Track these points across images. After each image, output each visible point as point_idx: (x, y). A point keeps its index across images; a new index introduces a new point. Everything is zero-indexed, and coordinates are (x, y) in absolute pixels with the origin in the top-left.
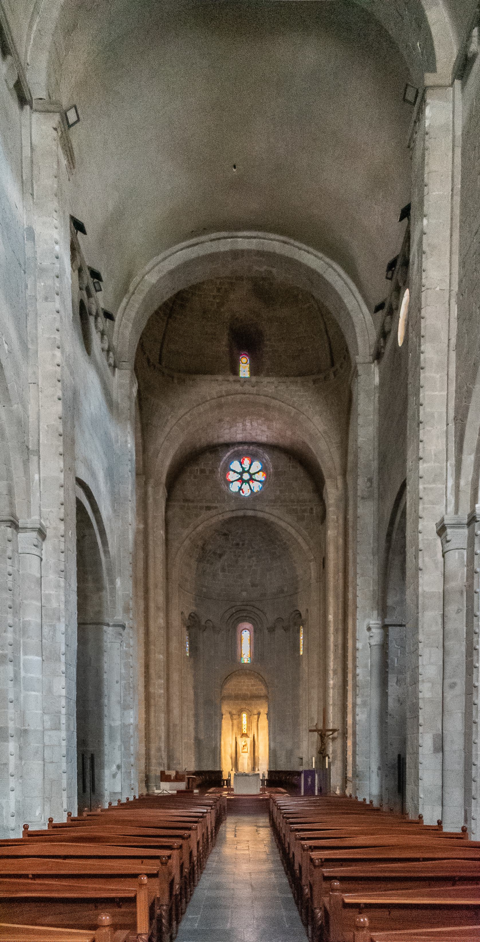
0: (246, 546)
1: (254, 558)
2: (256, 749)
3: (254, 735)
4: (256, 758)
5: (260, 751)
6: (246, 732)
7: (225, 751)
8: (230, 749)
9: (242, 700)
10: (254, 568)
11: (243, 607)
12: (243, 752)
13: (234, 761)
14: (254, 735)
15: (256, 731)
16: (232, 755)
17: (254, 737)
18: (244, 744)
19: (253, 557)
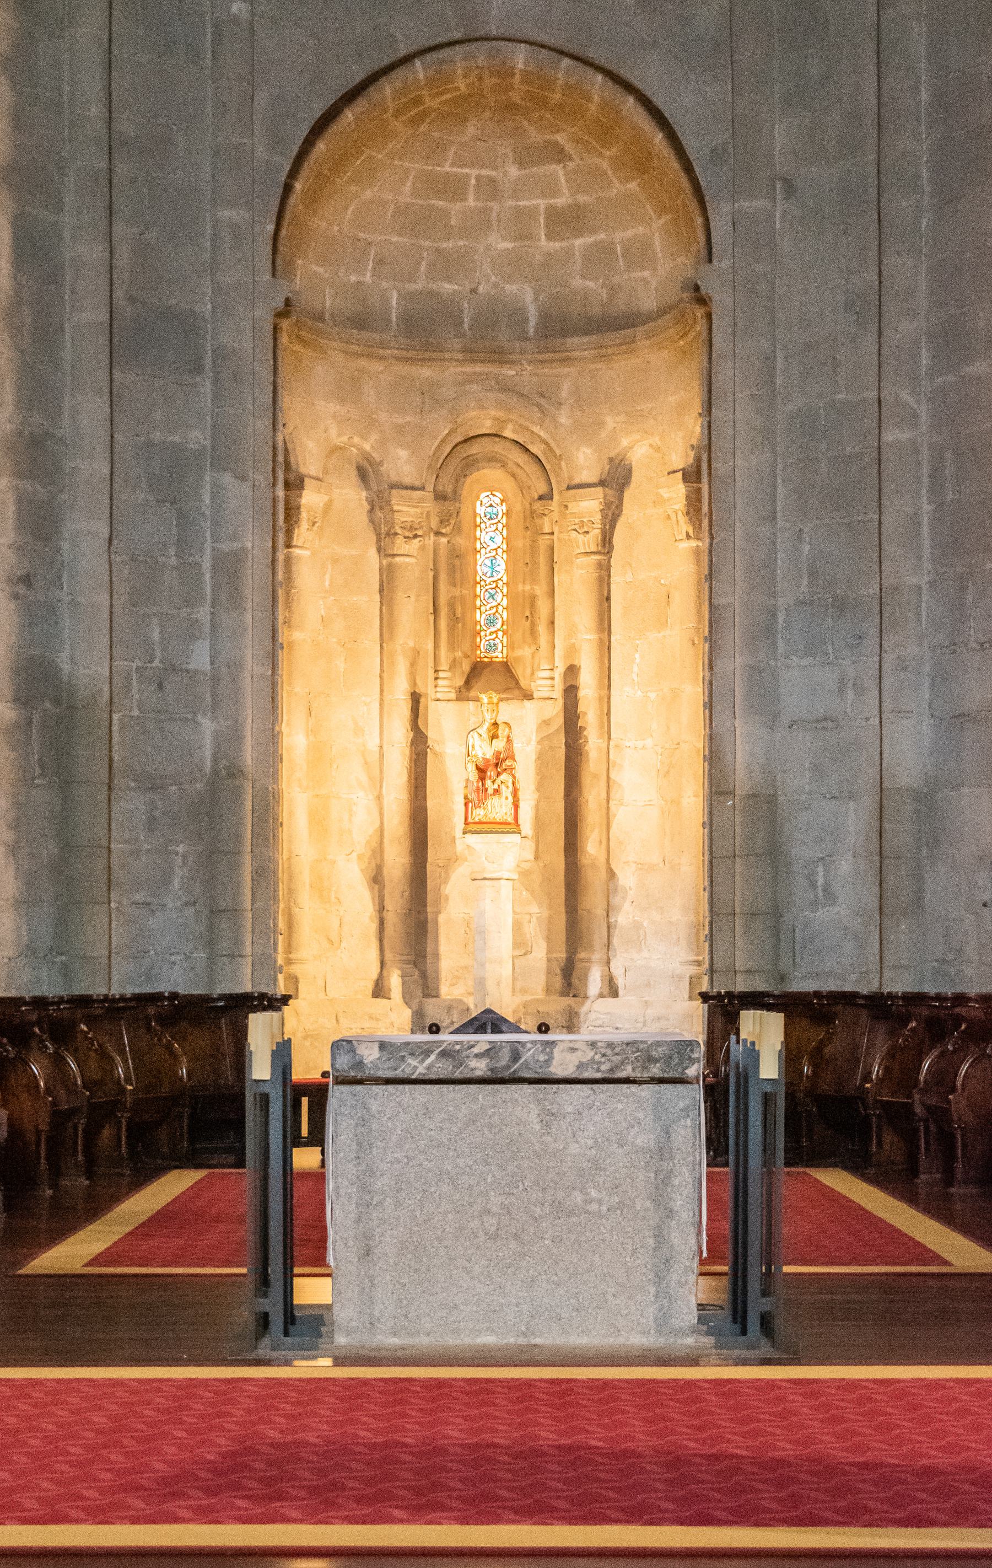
2: (592, 797)
3: (572, 671)
4: (594, 879)
5: (622, 817)
6: (498, 656)
7: (319, 821)
8: (362, 801)
9: (471, 354)
12: (471, 827)
13: (396, 903)
14: (572, 671)
15: (587, 638)
16: (378, 851)
17: (571, 692)
18: (484, 750)
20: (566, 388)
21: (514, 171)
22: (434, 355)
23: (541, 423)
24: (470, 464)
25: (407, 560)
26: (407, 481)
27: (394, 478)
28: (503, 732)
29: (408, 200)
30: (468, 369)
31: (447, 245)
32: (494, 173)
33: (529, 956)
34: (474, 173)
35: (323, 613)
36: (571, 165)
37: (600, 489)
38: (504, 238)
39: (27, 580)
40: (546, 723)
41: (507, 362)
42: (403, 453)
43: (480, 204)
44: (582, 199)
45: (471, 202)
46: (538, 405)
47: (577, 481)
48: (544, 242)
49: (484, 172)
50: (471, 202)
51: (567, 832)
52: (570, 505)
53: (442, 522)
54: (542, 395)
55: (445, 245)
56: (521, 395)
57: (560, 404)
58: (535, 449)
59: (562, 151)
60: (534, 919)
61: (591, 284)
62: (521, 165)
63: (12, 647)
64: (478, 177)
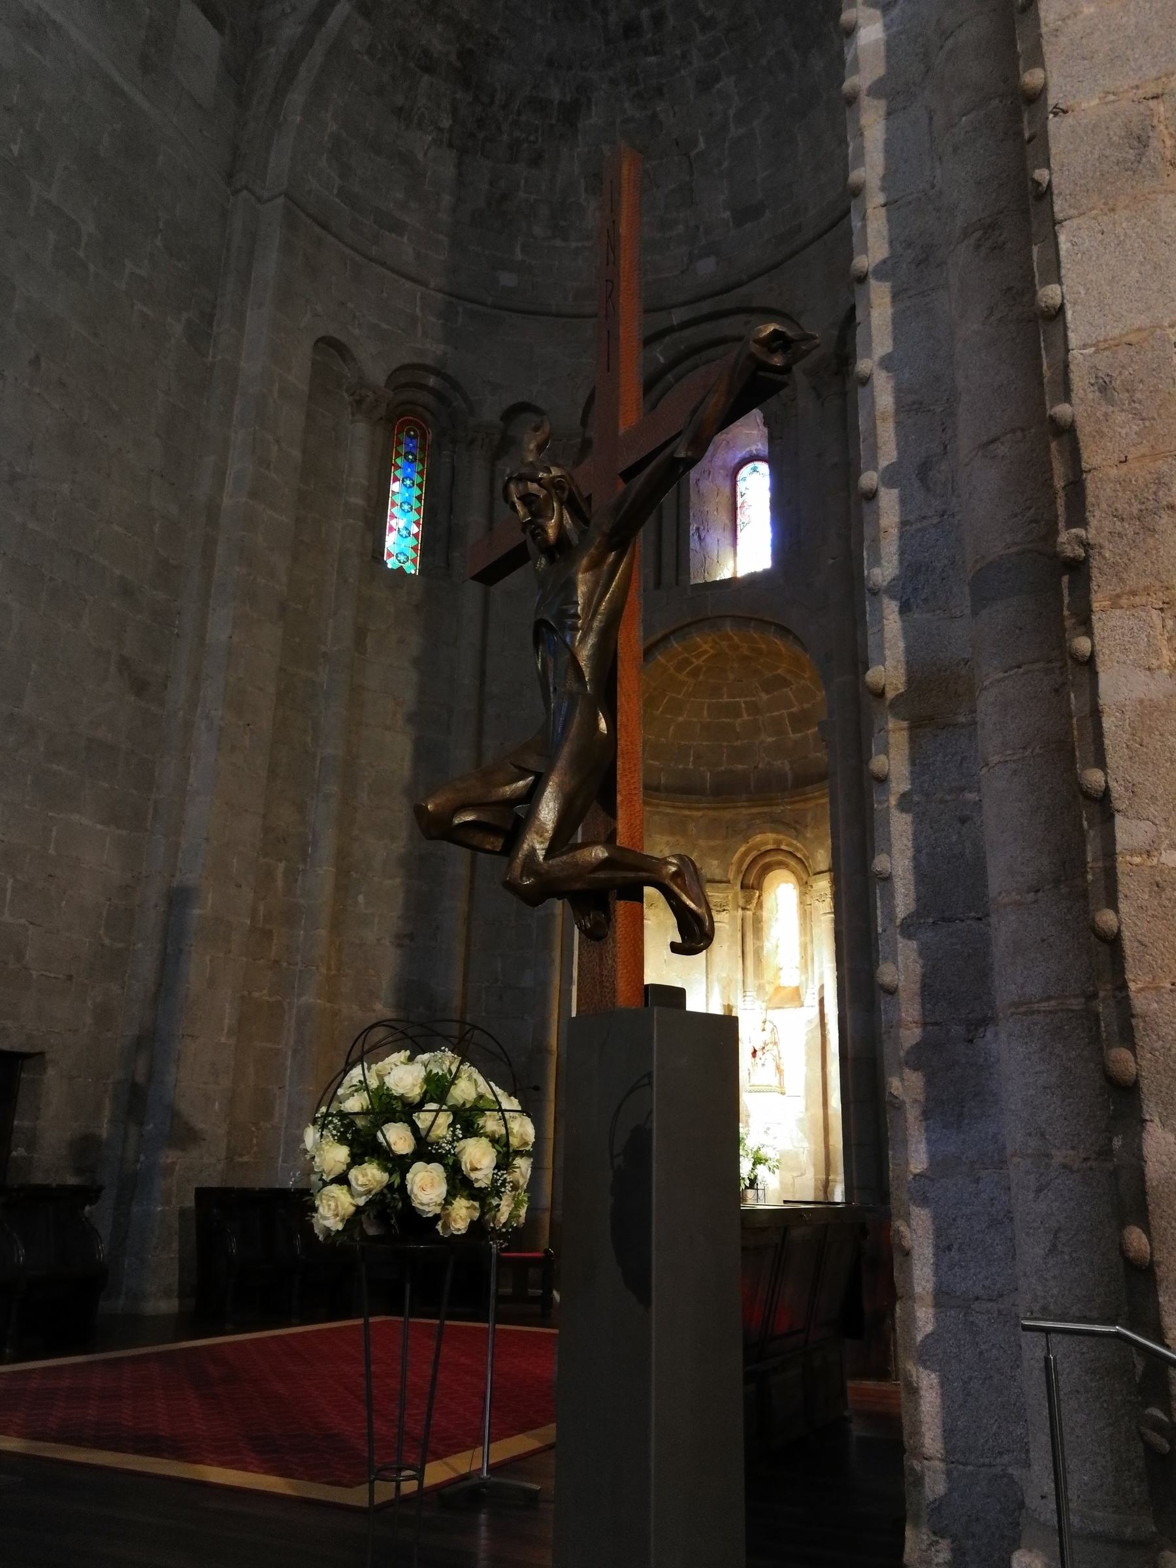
0: (671, 21)
1: (727, 83)
3: (822, 987)
10: (734, 131)
11: (707, 331)
14: (822, 987)
19: (717, 79)
20: (810, 815)
21: (765, 697)
22: (731, 805)
23: (796, 838)
24: (767, 868)
25: (723, 925)
26: (718, 878)
27: (709, 876)
28: (768, 1027)
29: (708, 720)
30: (754, 811)
31: (738, 743)
32: (754, 699)
33: (804, 1177)
34: (742, 700)
35: (665, 957)
36: (794, 687)
37: (828, 874)
38: (769, 736)
39: (411, 937)
40: (810, 1022)
41: (774, 805)
42: (715, 862)
43: (751, 718)
44: (806, 706)
45: (746, 717)
46: (795, 829)
47: (818, 870)
48: (791, 735)
49: (748, 699)
50: (746, 717)
51: (823, 1093)
52: (814, 885)
53: (747, 902)
54: (796, 822)
55: (735, 744)
56: (784, 823)
57: (807, 826)
58: (799, 855)
59: (785, 680)
60: (806, 1152)
61: (819, 754)
62: (767, 692)
63: (396, 975)
64: (745, 702)
